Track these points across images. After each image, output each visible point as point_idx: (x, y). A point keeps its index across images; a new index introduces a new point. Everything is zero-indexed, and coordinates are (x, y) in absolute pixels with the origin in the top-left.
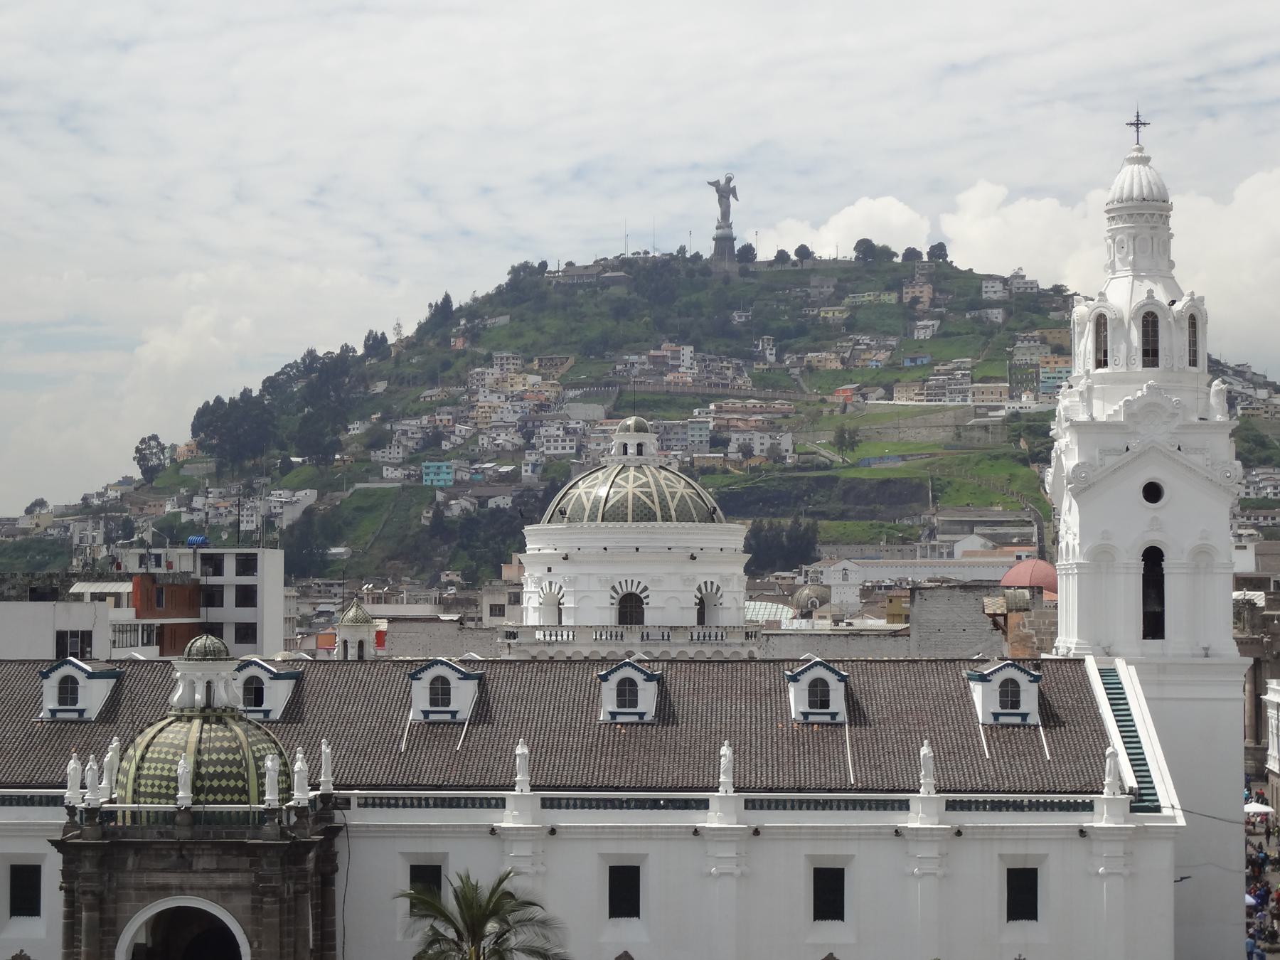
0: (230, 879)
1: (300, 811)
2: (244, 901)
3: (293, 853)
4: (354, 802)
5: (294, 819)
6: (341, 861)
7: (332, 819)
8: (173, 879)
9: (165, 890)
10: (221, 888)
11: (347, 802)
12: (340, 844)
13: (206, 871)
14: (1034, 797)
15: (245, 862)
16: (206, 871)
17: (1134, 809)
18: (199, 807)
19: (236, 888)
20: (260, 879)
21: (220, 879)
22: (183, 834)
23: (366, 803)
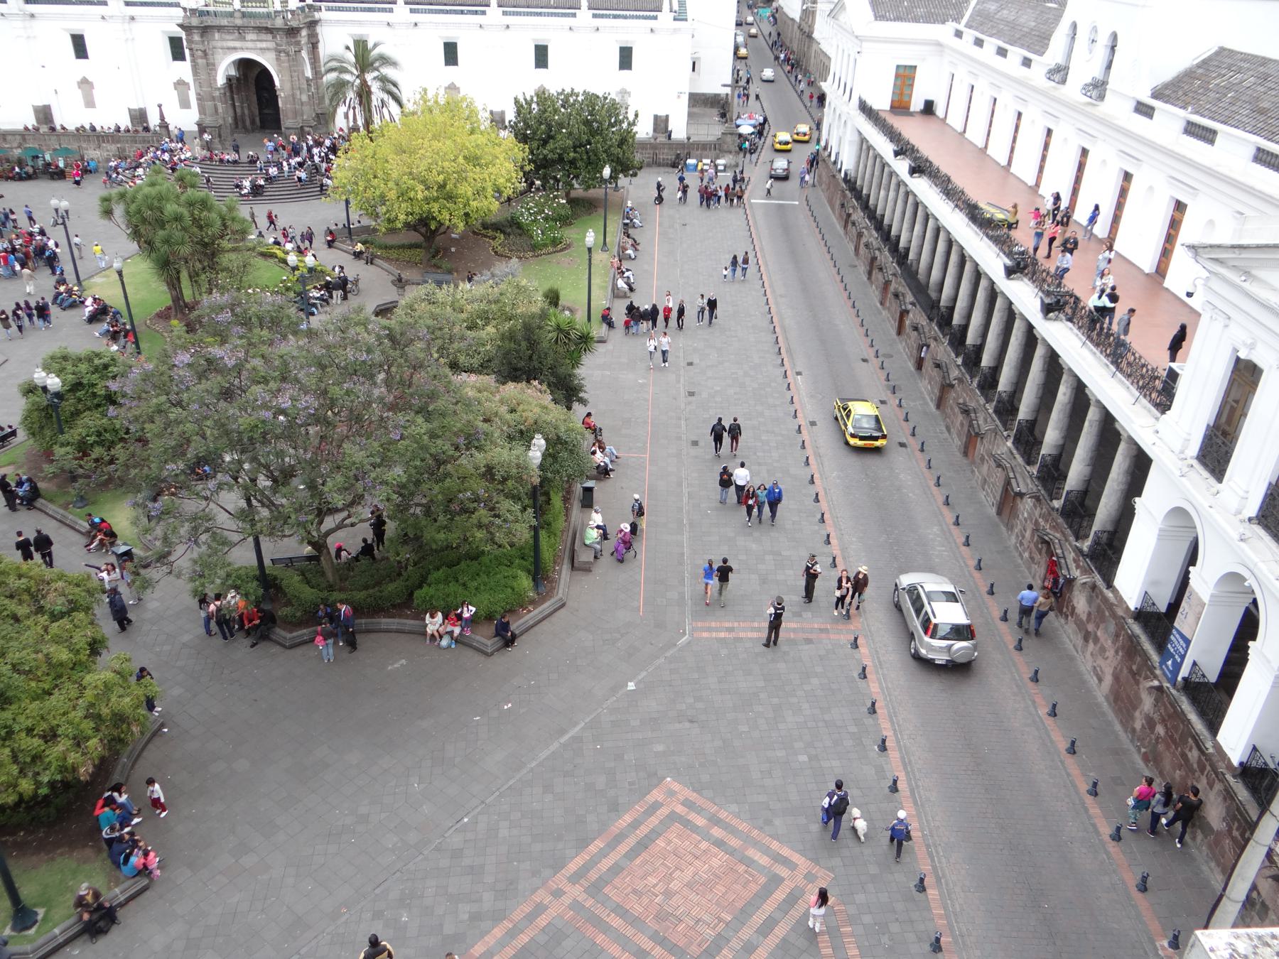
0: (264, 45)
1: (293, 12)
2: (272, 55)
3: (292, 32)
4: (323, 8)
5: (290, 16)
6: (320, 37)
7: (313, 16)
8: (237, 44)
9: (235, 49)
10: (261, 49)
11: (320, 9)
12: (319, 29)
13: (252, 41)
14: (632, 13)
15: (269, 37)
16: (252, 41)
17: (675, 19)
18: (244, 9)
19: (268, 49)
20: (277, 44)
21: (260, 45)
22: (239, 22)
23: (328, 9)
